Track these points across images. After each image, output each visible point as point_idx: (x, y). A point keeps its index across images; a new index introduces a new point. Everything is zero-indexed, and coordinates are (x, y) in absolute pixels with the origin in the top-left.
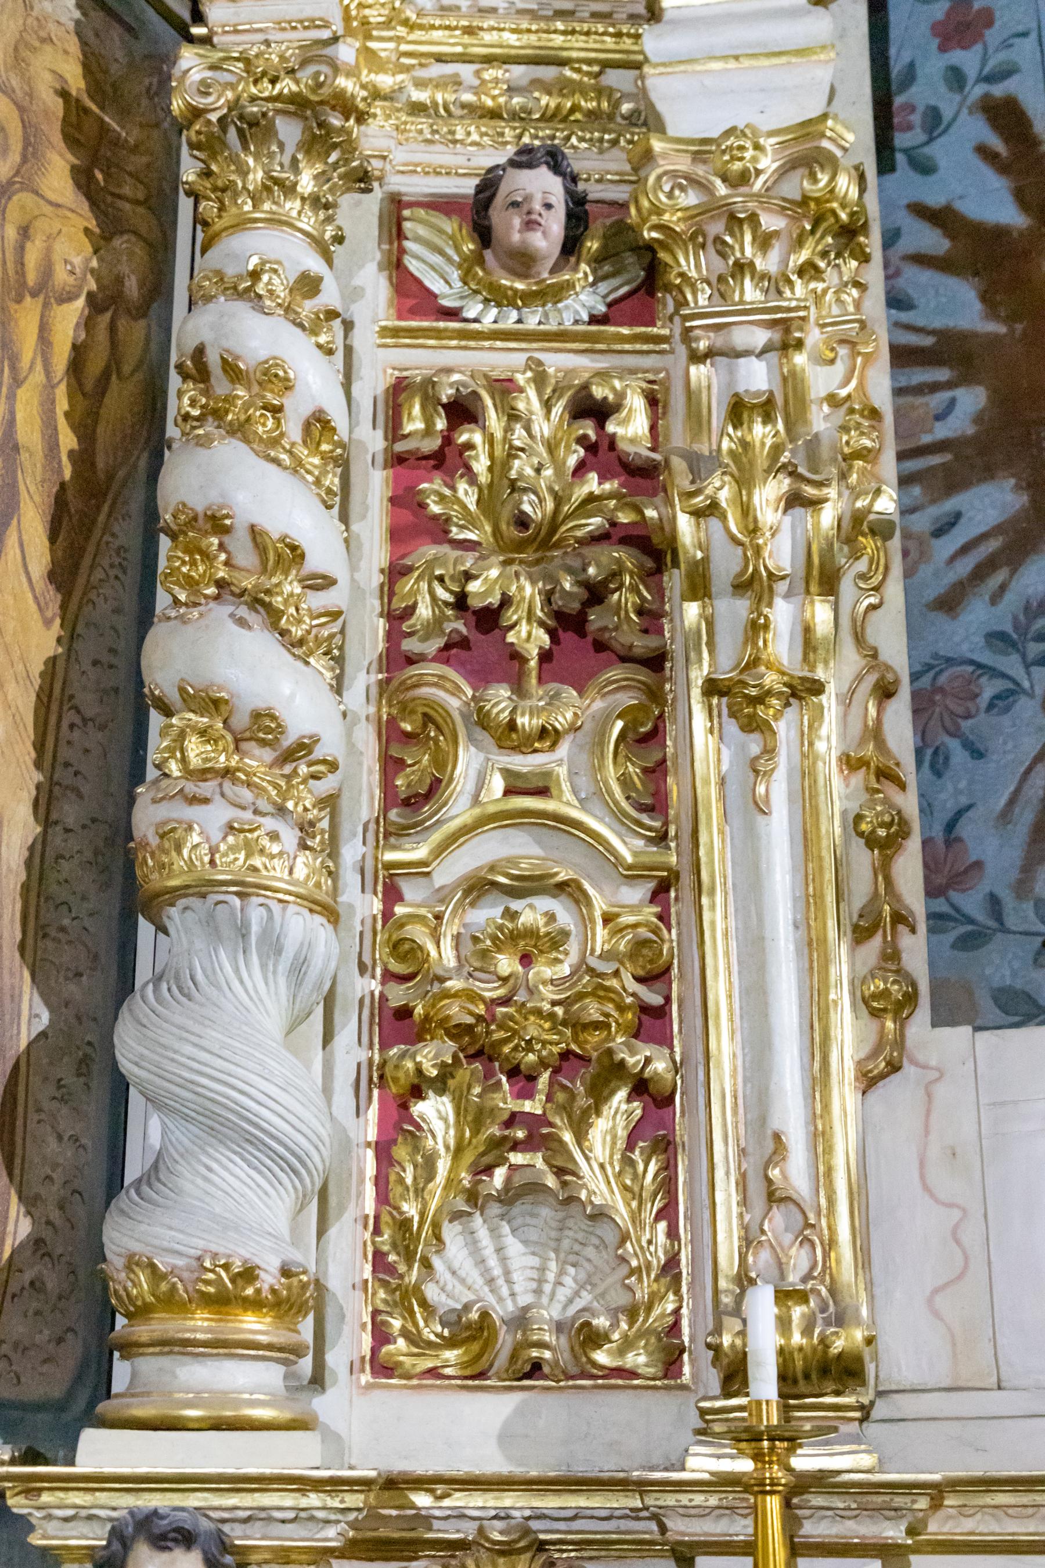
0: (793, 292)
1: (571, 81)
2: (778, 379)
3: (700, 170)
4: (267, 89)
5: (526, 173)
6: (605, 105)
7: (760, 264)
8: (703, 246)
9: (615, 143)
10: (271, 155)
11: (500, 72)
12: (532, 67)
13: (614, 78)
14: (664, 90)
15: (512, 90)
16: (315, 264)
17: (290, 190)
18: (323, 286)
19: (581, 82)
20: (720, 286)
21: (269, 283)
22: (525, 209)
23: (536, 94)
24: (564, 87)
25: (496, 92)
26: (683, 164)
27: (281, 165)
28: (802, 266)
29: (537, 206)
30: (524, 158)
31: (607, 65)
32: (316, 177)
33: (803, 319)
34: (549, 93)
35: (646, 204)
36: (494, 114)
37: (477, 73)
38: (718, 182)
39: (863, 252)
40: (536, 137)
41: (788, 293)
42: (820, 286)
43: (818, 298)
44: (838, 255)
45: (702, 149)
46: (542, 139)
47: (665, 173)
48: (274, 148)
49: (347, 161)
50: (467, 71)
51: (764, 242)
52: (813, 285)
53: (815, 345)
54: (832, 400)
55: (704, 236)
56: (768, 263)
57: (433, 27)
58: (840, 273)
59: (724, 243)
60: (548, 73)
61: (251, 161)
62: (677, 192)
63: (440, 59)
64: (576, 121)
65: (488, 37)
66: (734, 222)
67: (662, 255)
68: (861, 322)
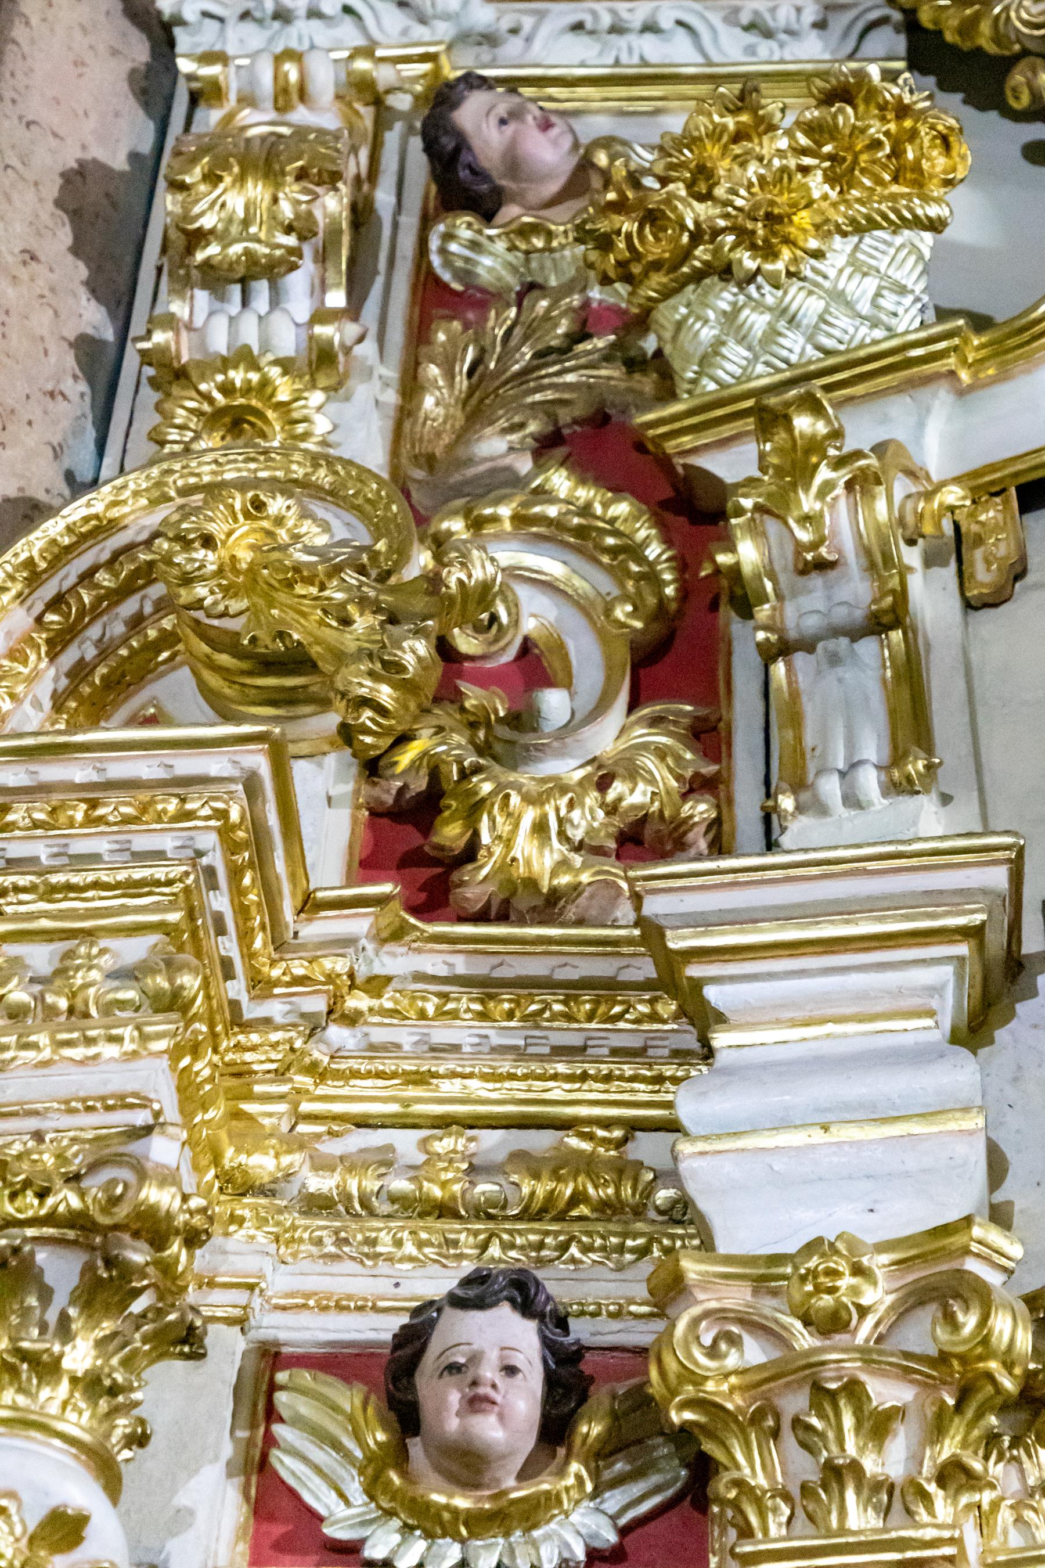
0: (931, 1512)
1: (581, 1153)
3: (768, 1307)
4: (30, 1205)
5: (476, 1318)
6: (627, 1191)
7: (871, 1465)
8: (775, 1433)
9: (643, 1252)
10: (25, 1312)
11: (462, 1141)
12: (514, 1132)
14: (706, 1171)
17: (47, 1368)
18: (89, 1531)
20: (809, 1499)
22: (469, 1377)
23: (515, 1178)
24: (563, 1164)
25: (450, 1175)
26: (737, 1297)
27: (43, 1328)
29: (489, 1372)
30: (472, 1293)
31: (634, 1127)
34: (536, 1176)
35: (672, 1366)
36: (444, 1210)
37: (424, 1143)
38: (798, 1325)
40: (512, 1246)
43: (984, 1519)
44: (1015, 1442)
45: (765, 1273)
46: (522, 1248)
47: (707, 1314)
48: (32, 1301)
49: (160, 1313)
50: (406, 1143)
51: (878, 1426)
55: (777, 1417)
56: (890, 1461)
57: (356, 1074)
59: (809, 1428)
60: (540, 1141)
62: (723, 1346)
63: (363, 1123)
64: (581, 1218)
65: (449, 1087)
66: (822, 1397)
67: (709, 1447)
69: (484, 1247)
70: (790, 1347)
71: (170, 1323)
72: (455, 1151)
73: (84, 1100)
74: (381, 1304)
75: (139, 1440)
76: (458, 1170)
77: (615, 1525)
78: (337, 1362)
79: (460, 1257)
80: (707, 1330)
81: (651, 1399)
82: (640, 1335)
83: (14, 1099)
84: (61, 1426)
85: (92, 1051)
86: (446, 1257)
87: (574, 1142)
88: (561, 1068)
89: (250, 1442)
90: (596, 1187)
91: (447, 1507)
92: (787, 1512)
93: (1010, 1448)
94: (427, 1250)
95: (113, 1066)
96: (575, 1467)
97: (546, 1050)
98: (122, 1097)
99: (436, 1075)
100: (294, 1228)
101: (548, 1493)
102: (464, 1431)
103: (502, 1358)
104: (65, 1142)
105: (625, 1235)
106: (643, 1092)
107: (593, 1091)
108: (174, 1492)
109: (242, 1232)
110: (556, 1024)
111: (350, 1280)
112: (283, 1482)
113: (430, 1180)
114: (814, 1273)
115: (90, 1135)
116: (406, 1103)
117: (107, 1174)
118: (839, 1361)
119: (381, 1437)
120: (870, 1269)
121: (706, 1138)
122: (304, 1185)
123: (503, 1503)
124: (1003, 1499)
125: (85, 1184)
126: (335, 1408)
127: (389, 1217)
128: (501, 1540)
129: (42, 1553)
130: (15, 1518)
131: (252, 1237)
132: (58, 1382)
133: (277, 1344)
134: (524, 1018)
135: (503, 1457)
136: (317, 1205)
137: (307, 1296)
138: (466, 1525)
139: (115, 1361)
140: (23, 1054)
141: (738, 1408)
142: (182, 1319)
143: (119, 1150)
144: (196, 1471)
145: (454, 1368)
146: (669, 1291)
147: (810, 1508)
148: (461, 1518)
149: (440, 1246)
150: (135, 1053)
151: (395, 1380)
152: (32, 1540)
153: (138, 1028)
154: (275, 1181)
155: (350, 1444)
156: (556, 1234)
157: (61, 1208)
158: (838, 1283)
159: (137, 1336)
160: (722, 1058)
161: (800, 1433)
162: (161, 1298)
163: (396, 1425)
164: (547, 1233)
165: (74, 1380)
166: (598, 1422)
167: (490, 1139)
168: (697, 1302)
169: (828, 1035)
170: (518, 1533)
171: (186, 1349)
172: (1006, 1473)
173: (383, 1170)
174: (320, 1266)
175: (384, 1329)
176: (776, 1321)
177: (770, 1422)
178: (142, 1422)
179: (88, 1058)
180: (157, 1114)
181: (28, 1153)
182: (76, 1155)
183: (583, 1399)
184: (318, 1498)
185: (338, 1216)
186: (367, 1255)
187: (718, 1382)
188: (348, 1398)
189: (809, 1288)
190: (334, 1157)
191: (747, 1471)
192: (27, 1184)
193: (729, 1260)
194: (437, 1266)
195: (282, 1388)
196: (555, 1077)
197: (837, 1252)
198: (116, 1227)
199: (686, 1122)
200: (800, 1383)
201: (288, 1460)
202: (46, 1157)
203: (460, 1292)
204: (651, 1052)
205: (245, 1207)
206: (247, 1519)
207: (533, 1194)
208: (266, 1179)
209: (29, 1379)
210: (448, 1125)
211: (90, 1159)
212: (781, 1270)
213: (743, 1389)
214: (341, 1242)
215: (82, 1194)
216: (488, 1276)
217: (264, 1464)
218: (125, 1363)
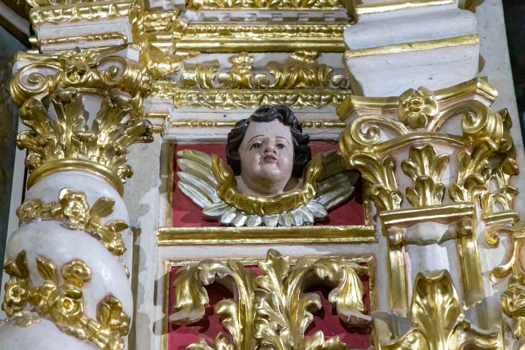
1: (298, 62)
2: (456, 259)
3: (389, 118)
4: (76, 78)
5: (263, 125)
7: (435, 179)
8: (394, 169)
9: (329, 101)
10: (79, 122)
11: (247, 59)
12: (269, 54)
13: (326, 59)
15: (254, 69)
16: (108, 192)
17: (91, 144)
18: (115, 208)
19: (304, 63)
20: (409, 195)
21: (75, 207)
23: (272, 72)
24: (291, 66)
25: (244, 71)
26: (376, 115)
27: (87, 128)
28: (467, 179)
29: (272, 146)
30: (262, 115)
32: (110, 134)
33: (471, 216)
34: (281, 71)
35: (350, 142)
36: (243, 86)
37: (231, 60)
38: (402, 125)
39: (513, 169)
40: (273, 99)
41: (458, 199)
42: (483, 193)
43: (482, 201)
44: (494, 171)
46: (277, 100)
47: (364, 121)
48: (81, 117)
50: (223, 59)
51: (438, 164)
52: (476, 193)
53: (482, 234)
54: (498, 272)
55: (395, 162)
56: (443, 178)
58: (497, 183)
59: (410, 166)
60: (281, 57)
61: (64, 126)
62: (372, 134)
63: (204, 51)
65: (238, 36)
66: (414, 152)
67: (365, 175)
68: (514, 216)
69: (261, 100)
70: (398, 133)
71: (139, 126)
72: (244, 62)
73: (94, 36)
74: (219, 124)
75: (128, 174)
76: (247, 69)
77: (325, 209)
78: (205, 147)
79: (252, 104)
80: (364, 128)
81: (340, 158)
82: (333, 134)
83: (63, 36)
84: (99, 167)
85: (95, 15)
86: (245, 104)
87: (295, 57)
88: (288, 27)
89: (168, 179)
90: (307, 75)
91: (256, 202)
92: (401, 200)
93: (492, 174)
94: (236, 102)
95: (104, 21)
96: (308, 185)
97: (281, 19)
98: (111, 34)
99: (233, 31)
100: (180, 94)
101: (297, 195)
102: (263, 171)
103: (277, 141)
104: (89, 52)
105: (321, 94)
106: (323, 36)
107: (303, 37)
108: (139, 198)
109: (158, 95)
110: (285, 8)
111: (205, 114)
112: (184, 195)
113: (236, 73)
114: (409, 103)
115: (98, 50)
116: (222, 42)
117: (108, 65)
118: (419, 138)
119: (226, 174)
120: (433, 101)
121: (359, 51)
122: (182, 76)
123: (279, 200)
124: (490, 194)
125: (99, 69)
126: (204, 165)
127: (219, 88)
128: (278, 215)
129: (96, 216)
130: (85, 202)
131: (163, 97)
132: (96, 150)
133: (175, 140)
134: (271, 6)
135: (279, 181)
136: (188, 84)
137: (188, 121)
138: (263, 209)
139: (117, 141)
140: (65, 17)
141: (378, 158)
142: (144, 125)
143: (113, 54)
144: (148, 191)
145: (257, 146)
146: (349, 112)
147: (410, 198)
148: (262, 206)
149: (242, 100)
150: (114, 16)
151: (230, 151)
152: (91, 212)
153: (115, 5)
154: (170, 74)
155: (212, 178)
156: (291, 94)
157: (90, 79)
158: (420, 107)
159: (125, 132)
160: (361, 19)
161: (405, 169)
162: (132, 118)
163: (232, 170)
164: (287, 94)
165: (101, 149)
166: (318, 167)
167: (259, 57)
168: (359, 117)
169: (407, 8)
170: (285, 212)
171: (145, 138)
172: (490, 184)
173: (215, 69)
174: (192, 109)
175: (223, 134)
176: (393, 124)
177: (392, 165)
178: (129, 167)
179: (94, 18)
180: (126, 41)
181: (74, 56)
182: (94, 57)
183: (310, 159)
184: (199, 200)
185: (197, 89)
186: (211, 104)
187: (370, 149)
188: (210, 160)
189: (407, 109)
190: (193, 64)
191: (383, 184)
192: (75, 69)
193: (372, 99)
194: (241, 108)
195: (180, 157)
196: (285, 31)
197: (419, 95)
198: (115, 86)
199: (349, 45)
200: (405, 148)
201: (185, 186)
202: (82, 58)
203: (257, 115)
204: (326, 19)
205: (159, 85)
206: (170, 210)
207: (280, 78)
208: (166, 73)
209: (84, 148)
210: (240, 52)
211: (100, 59)
212: (394, 103)
213: (379, 151)
214: (199, 99)
215: (98, 74)
216: (268, 109)
217: (175, 188)
218: (121, 142)
